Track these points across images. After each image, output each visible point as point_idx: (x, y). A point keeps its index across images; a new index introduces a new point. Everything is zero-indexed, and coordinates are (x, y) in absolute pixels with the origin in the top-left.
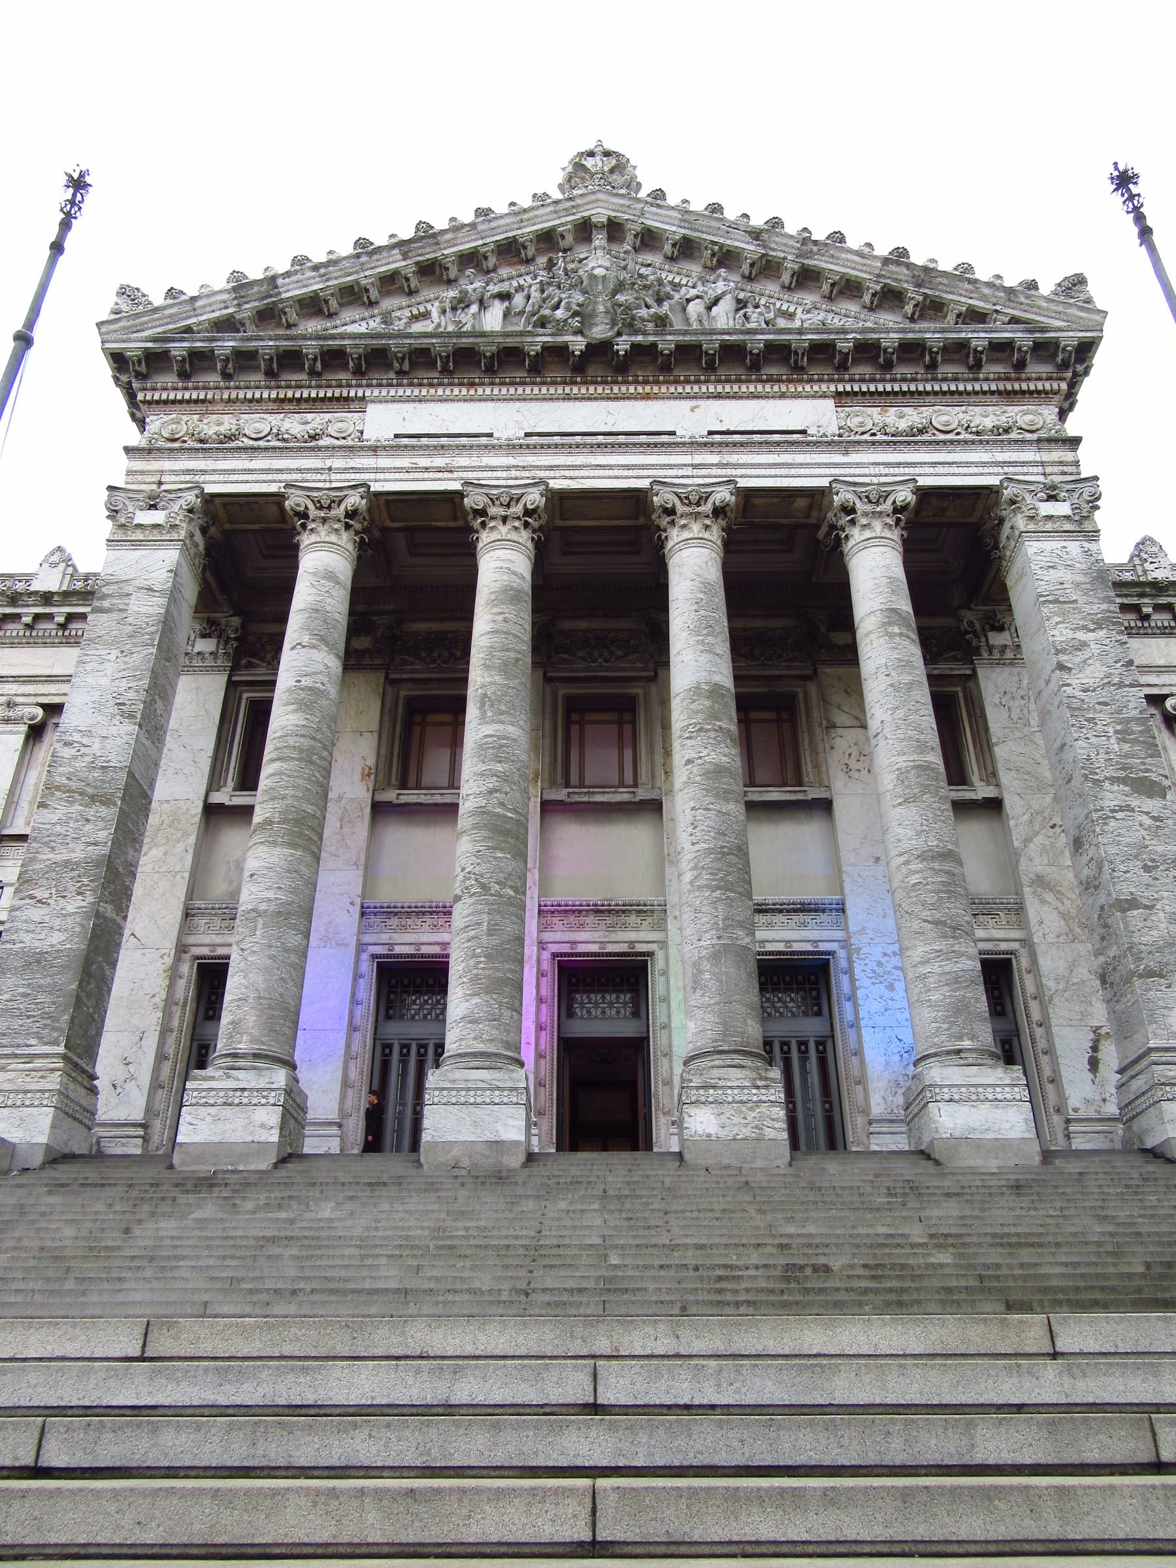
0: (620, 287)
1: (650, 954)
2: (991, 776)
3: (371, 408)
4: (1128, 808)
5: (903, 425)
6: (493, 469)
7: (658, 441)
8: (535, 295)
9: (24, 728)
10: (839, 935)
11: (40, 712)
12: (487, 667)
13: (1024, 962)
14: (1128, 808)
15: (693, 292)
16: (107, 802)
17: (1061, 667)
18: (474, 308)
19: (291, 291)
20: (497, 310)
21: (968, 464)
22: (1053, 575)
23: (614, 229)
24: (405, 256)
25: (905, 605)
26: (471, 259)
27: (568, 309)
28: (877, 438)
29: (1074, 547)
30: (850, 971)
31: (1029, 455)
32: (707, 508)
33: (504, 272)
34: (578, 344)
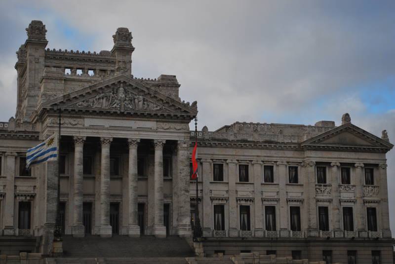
0: (125, 100)
1: (120, 202)
2: (172, 176)
3: (85, 119)
4: (184, 194)
5: (166, 128)
6: (104, 133)
7: (129, 129)
8: (111, 97)
9: (14, 157)
10: (146, 200)
11: (16, 154)
12: (105, 170)
13: (171, 205)
14: (184, 194)
15: (135, 97)
16: (56, 189)
17: (180, 173)
18: (101, 100)
19: (72, 96)
20: (105, 100)
21: (174, 136)
22: (182, 157)
23: (124, 82)
24: (90, 89)
25: (162, 161)
26: (101, 88)
27: (118, 105)
28: (162, 130)
29: (186, 152)
30: (147, 206)
31: (183, 135)
32: (136, 142)
33: (106, 89)
34: (119, 112)
